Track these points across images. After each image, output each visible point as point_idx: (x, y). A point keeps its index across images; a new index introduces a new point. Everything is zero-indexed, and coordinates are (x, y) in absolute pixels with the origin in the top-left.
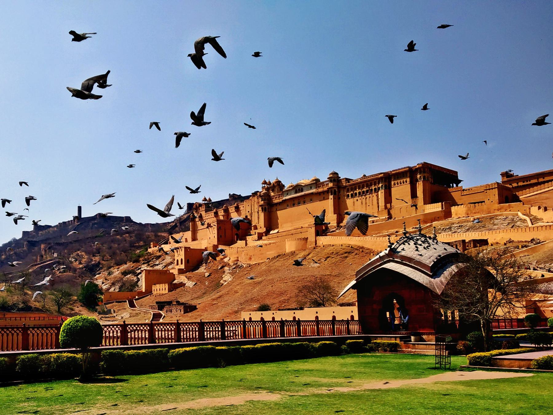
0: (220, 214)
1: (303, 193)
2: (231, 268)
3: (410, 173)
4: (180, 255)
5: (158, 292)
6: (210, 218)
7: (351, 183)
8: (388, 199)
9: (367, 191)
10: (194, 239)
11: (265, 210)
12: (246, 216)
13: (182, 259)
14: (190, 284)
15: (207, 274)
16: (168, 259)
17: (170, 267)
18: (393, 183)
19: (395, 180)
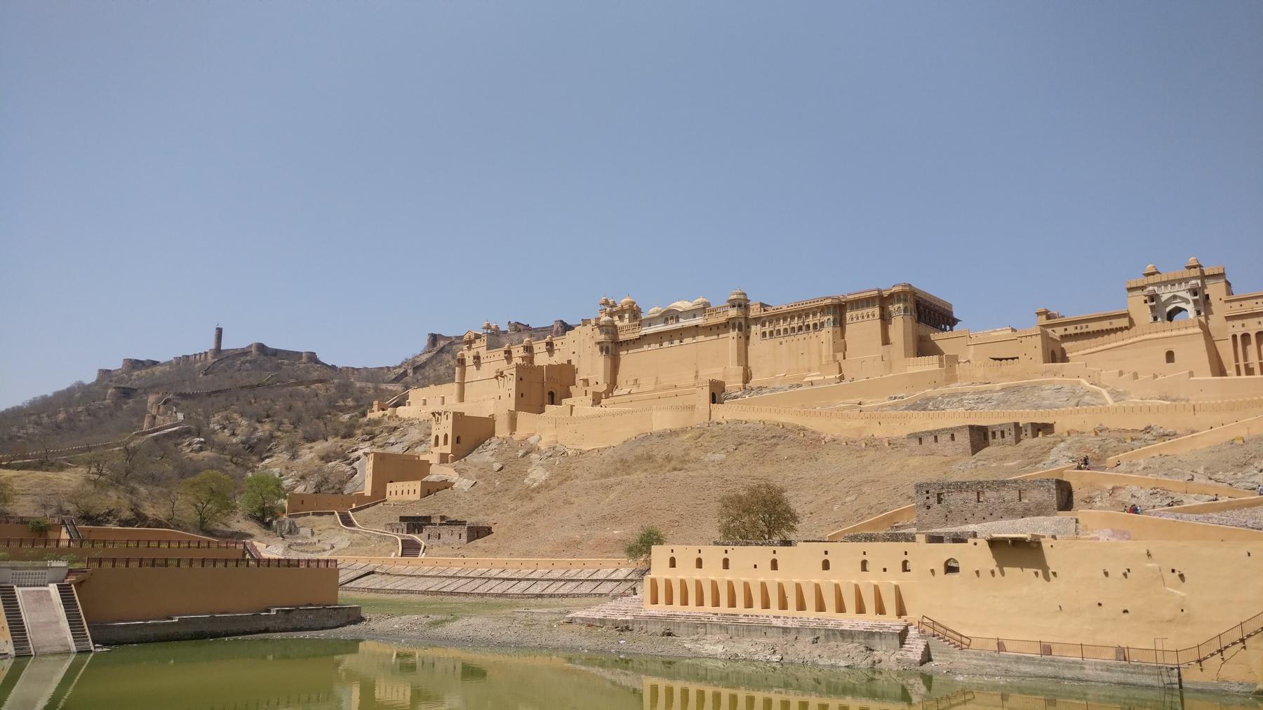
0: (514, 354)
1: (679, 325)
2: (544, 456)
3: (883, 301)
4: (445, 427)
5: (399, 496)
6: (494, 361)
7: (770, 311)
8: (840, 346)
9: (800, 328)
10: (461, 398)
11: (607, 352)
12: (569, 361)
13: (446, 436)
14: (463, 484)
15: (497, 466)
16: (415, 434)
17: (419, 449)
18: (848, 315)
19: (852, 309)
